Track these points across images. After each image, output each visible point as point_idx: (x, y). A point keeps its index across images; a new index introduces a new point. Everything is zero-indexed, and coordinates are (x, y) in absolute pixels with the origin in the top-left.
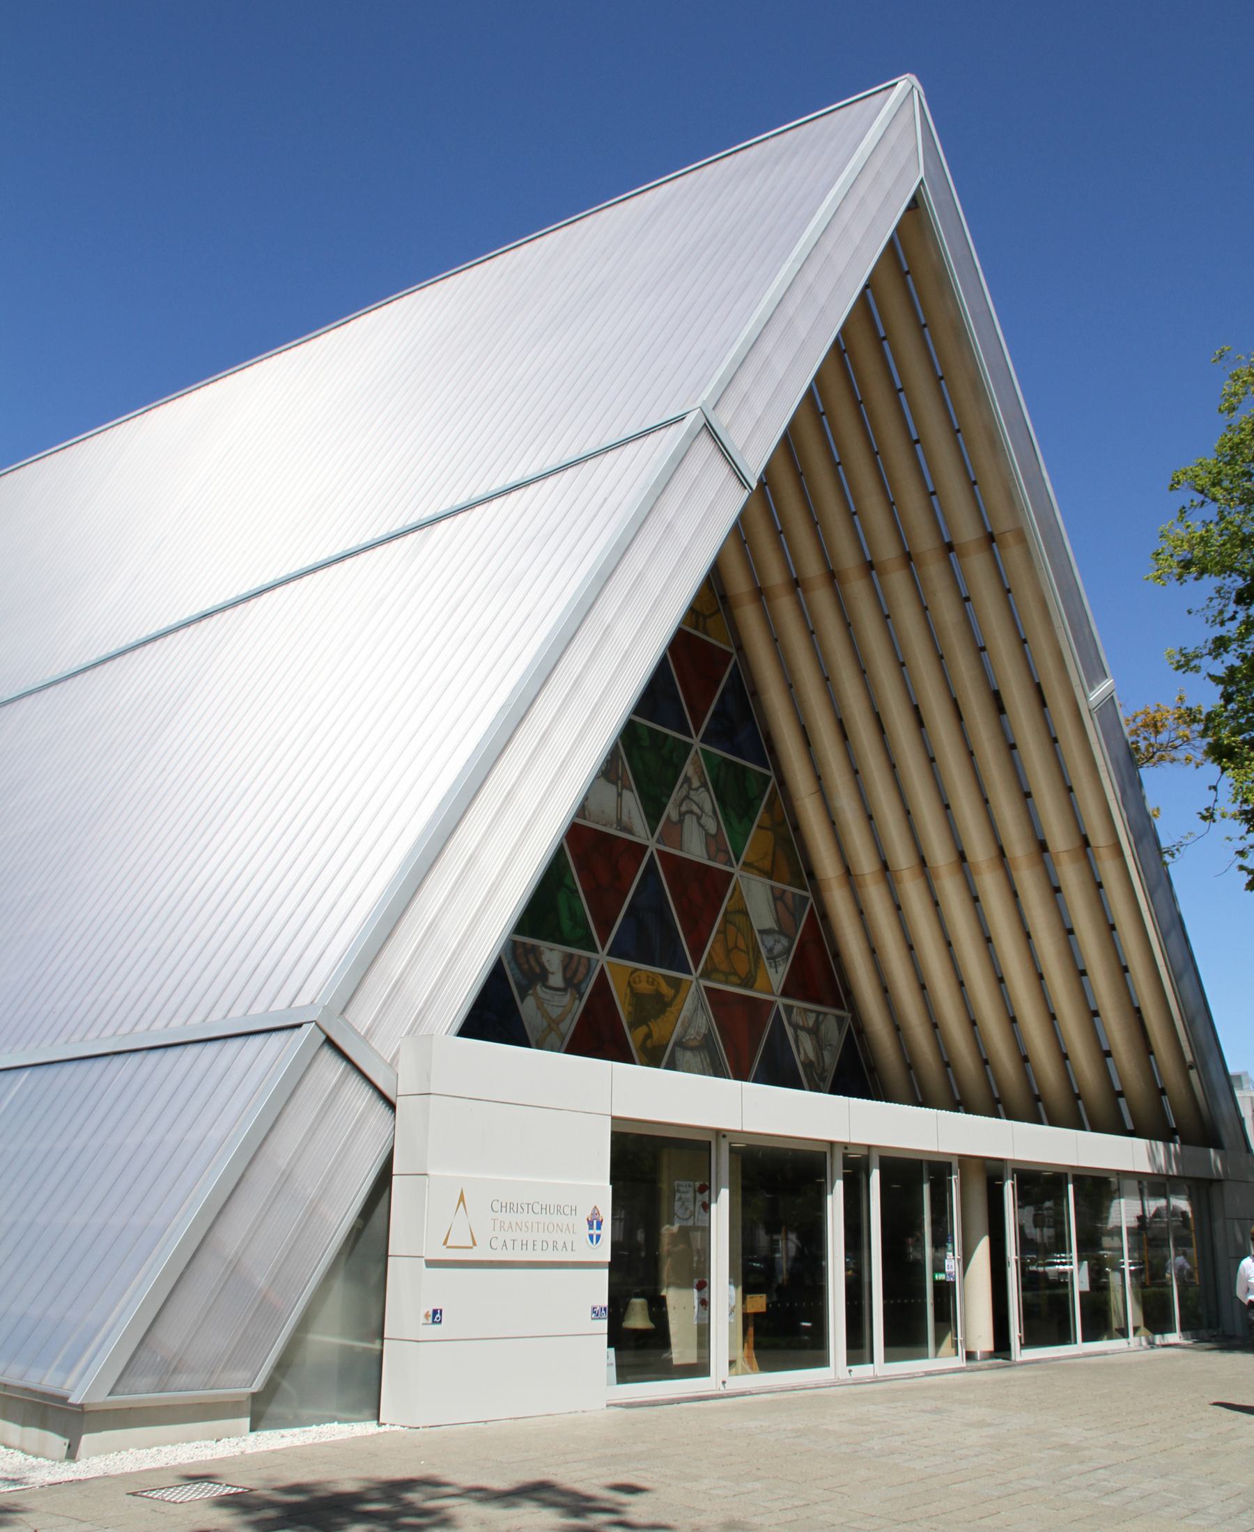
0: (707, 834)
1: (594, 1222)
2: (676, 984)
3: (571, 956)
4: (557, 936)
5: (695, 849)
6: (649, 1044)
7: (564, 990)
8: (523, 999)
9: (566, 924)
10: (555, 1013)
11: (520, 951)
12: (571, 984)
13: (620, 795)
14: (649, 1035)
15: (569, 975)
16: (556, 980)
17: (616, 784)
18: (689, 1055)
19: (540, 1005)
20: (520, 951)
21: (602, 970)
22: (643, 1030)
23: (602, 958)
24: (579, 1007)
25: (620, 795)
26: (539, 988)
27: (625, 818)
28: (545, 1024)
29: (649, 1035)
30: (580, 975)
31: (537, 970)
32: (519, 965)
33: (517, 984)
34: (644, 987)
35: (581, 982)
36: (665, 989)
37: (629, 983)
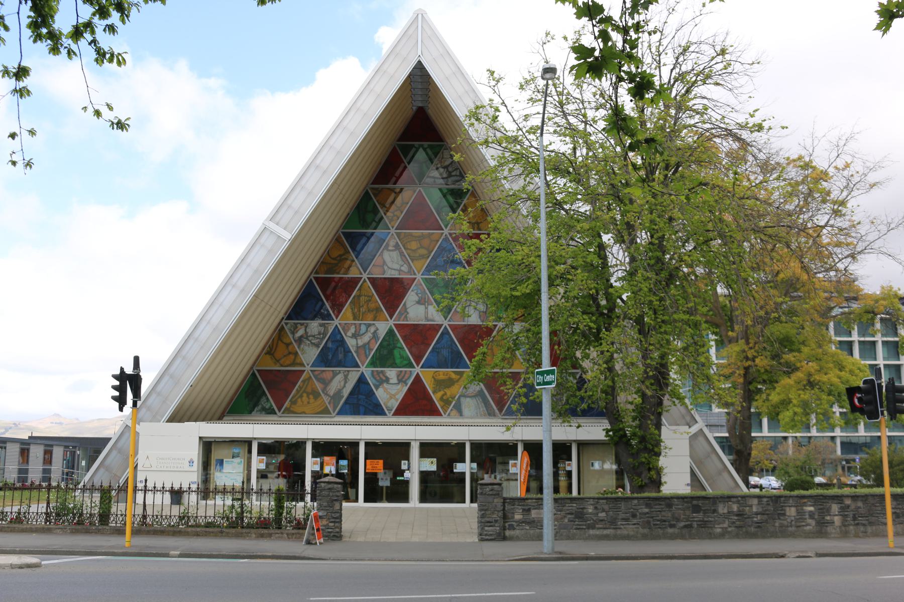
0: (480, 312)
1: (191, 462)
2: (461, 374)
3: (401, 371)
4: (393, 365)
5: (474, 319)
6: (445, 398)
7: (398, 384)
8: (377, 389)
9: (398, 361)
10: (393, 392)
11: (375, 373)
12: (401, 380)
13: (426, 308)
14: (445, 394)
15: (400, 378)
16: (394, 380)
17: (425, 304)
18: (468, 399)
19: (386, 390)
20: (375, 373)
21: (418, 374)
22: (440, 394)
23: (417, 370)
24: (406, 389)
25: (426, 308)
26: (385, 385)
27: (430, 316)
28: (388, 396)
29: (443, 395)
30: (406, 377)
31: (384, 378)
32: (375, 378)
33: (374, 385)
34: (442, 377)
35: (406, 380)
36: (453, 376)
37: (433, 377)
